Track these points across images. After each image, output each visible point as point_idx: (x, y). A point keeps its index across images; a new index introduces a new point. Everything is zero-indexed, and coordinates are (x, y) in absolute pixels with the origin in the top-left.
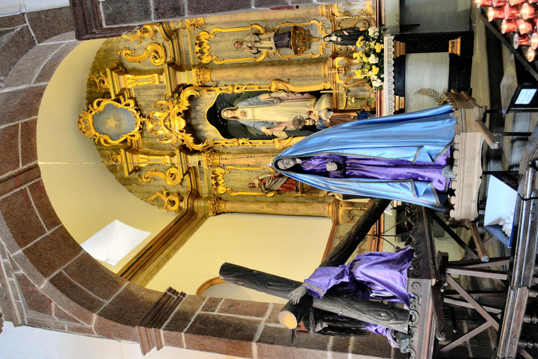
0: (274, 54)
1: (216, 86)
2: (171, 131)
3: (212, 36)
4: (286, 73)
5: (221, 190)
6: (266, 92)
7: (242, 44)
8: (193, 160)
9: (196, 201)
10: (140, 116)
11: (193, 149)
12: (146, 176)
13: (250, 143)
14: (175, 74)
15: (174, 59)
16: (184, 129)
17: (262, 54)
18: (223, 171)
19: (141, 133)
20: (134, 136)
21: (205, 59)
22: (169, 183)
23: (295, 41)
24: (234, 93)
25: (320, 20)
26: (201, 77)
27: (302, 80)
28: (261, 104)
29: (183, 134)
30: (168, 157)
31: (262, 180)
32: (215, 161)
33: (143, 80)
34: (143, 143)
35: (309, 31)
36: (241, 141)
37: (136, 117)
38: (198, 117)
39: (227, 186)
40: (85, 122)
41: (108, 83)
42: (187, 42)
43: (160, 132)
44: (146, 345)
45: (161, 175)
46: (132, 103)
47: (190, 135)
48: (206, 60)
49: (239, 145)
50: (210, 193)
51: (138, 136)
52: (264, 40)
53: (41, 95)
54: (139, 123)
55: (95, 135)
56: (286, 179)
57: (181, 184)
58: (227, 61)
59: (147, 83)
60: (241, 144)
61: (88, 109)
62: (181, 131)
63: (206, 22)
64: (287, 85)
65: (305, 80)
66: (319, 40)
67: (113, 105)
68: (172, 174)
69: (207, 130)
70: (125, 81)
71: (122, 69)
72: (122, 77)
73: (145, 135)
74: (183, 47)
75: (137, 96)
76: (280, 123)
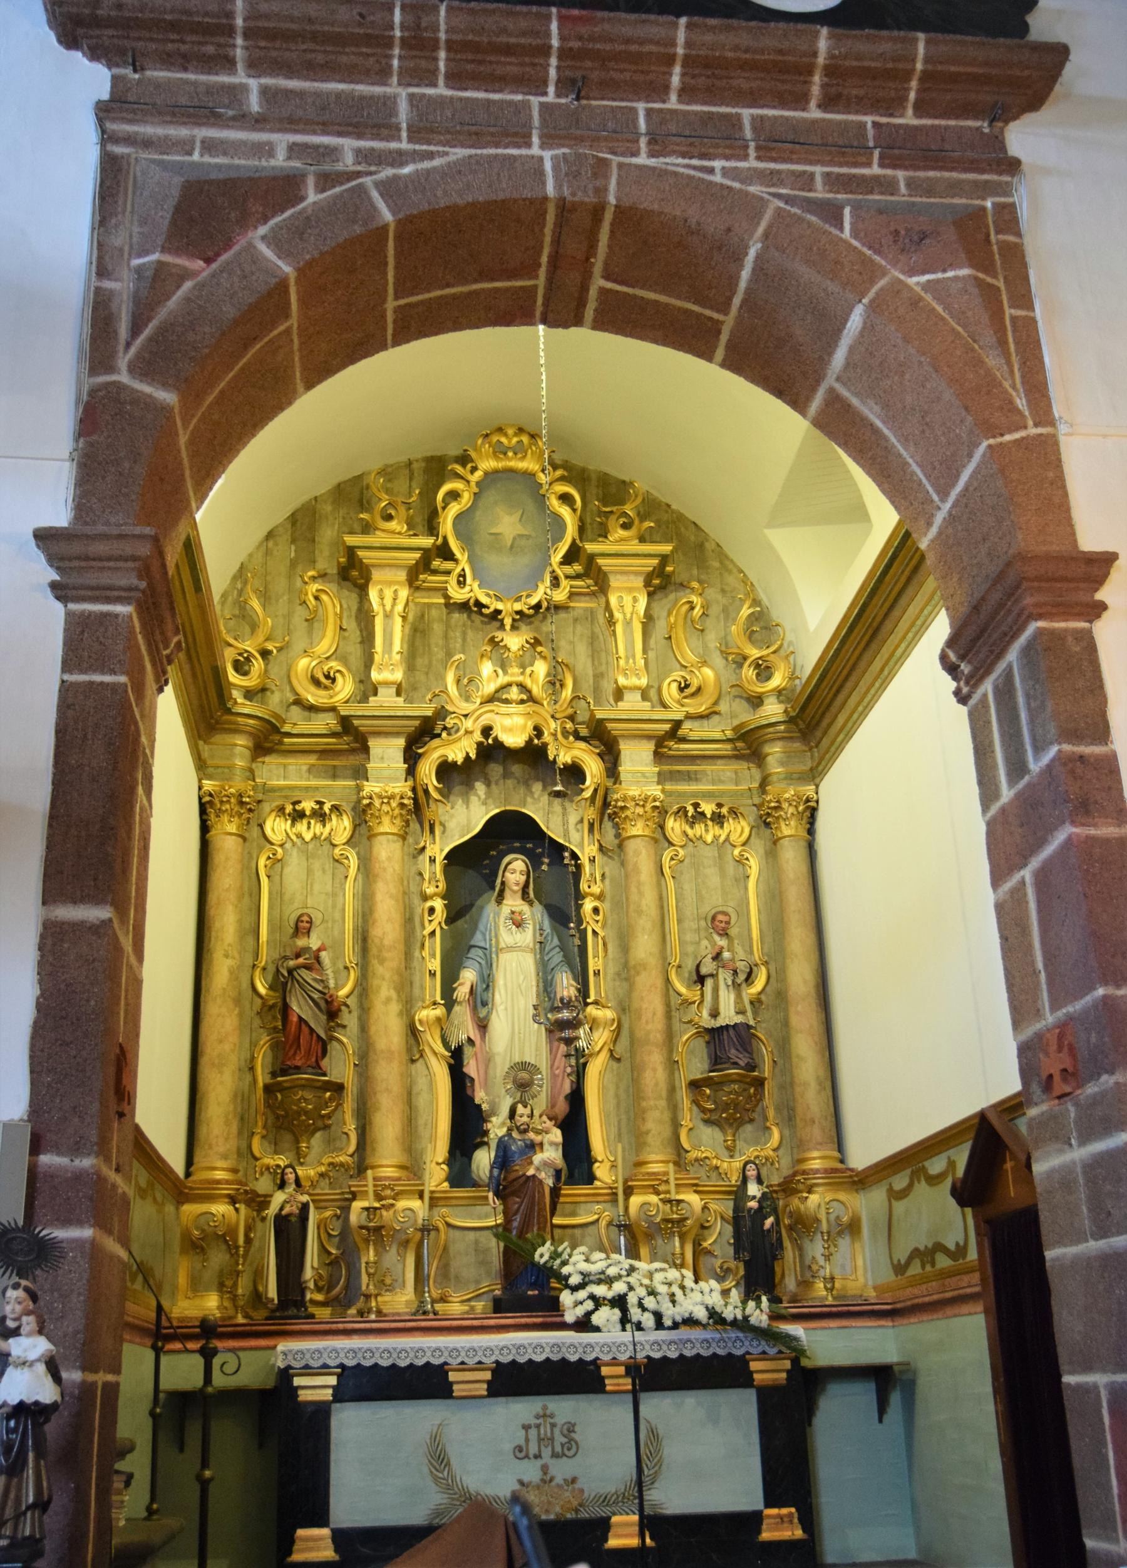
0: (690, 1022)
1: (601, 849)
2: (491, 699)
3: (736, 852)
5: (276, 828)
6: (584, 992)
7: (724, 934)
8: (387, 754)
9: (250, 744)
11: (420, 756)
12: (324, 597)
13: (433, 933)
14: (649, 737)
15: (684, 740)
16: (496, 739)
17: (688, 987)
18: (341, 837)
19: (464, 606)
20: (462, 582)
21: (677, 825)
22: (303, 663)
23: (733, 1081)
25: (781, 1152)
26: (640, 810)
27: (617, 1096)
28: (545, 973)
29: (478, 737)
30: (398, 675)
31: (318, 959)
32: (386, 820)
33: (628, 641)
34: (429, 605)
35: (751, 1121)
36: (438, 904)
37: (518, 599)
38: (510, 783)
39: (288, 845)
41: (622, 540)
42: (721, 782)
44: (77, 548)
45: (325, 645)
46: (560, 596)
47: (473, 756)
48: (674, 826)
49: (425, 898)
50: (267, 790)
51: (458, 595)
52: (739, 996)
53: (779, 393)
54: (500, 606)
57: (298, 702)
58: (671, 883)
59: (622, 652)
60: (429, 904)
62: (487, 731)
63: (785, 842)
64: (604, 1056)
65: (618, 1105)
66: (728, 1148)
68: (334, 680)
69: (471, 806)
70: (630, 590)
71: (660, 583)
72: (639, 582)
73: (456, 615)
74: (708, 768)
75: (573, 614)
76: (483, 1026)
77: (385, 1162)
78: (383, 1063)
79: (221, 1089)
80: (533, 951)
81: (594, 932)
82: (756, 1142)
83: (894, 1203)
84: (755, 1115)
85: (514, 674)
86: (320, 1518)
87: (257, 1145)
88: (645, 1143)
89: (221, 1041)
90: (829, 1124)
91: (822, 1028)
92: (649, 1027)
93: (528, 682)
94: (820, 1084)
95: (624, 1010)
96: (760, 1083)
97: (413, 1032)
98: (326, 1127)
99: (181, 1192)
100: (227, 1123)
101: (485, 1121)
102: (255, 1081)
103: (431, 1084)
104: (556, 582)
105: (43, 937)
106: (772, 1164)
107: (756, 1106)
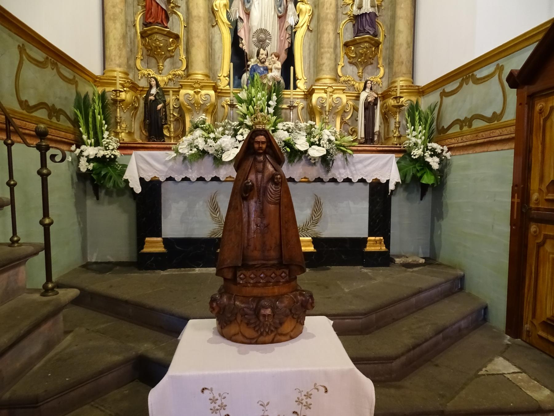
0: (346, 14)
4: (327, 24)
23: (366, 42)
25: (383, 79)
27: (309, 49)
35: (372, 64)
56: (164, 7)
64: (305, 27)
65: (310, 53)
66: (359, 76)
76: (248, 13)
77: (197, 72)
78: (195, 22)
79: (116, 31)
82: (372, 75)
83: (444, 97)
84: (373, 61)
86: (159, 235)
87: (139, 63)
88: (321, 70)
89: (114, 7)
90: (410, 65)
91: (412, 17)
92: (328, 11)
94: (408, 44)
95: (315, 6)
96: (377, 44)
97: (213, 12)
98: (172, 57)
99: (95, 80)
100: (120, 49)
101: (248, 61)
102: (136, 32)
103: (221, 39)
106: (379, 85)
107: (374, 57)
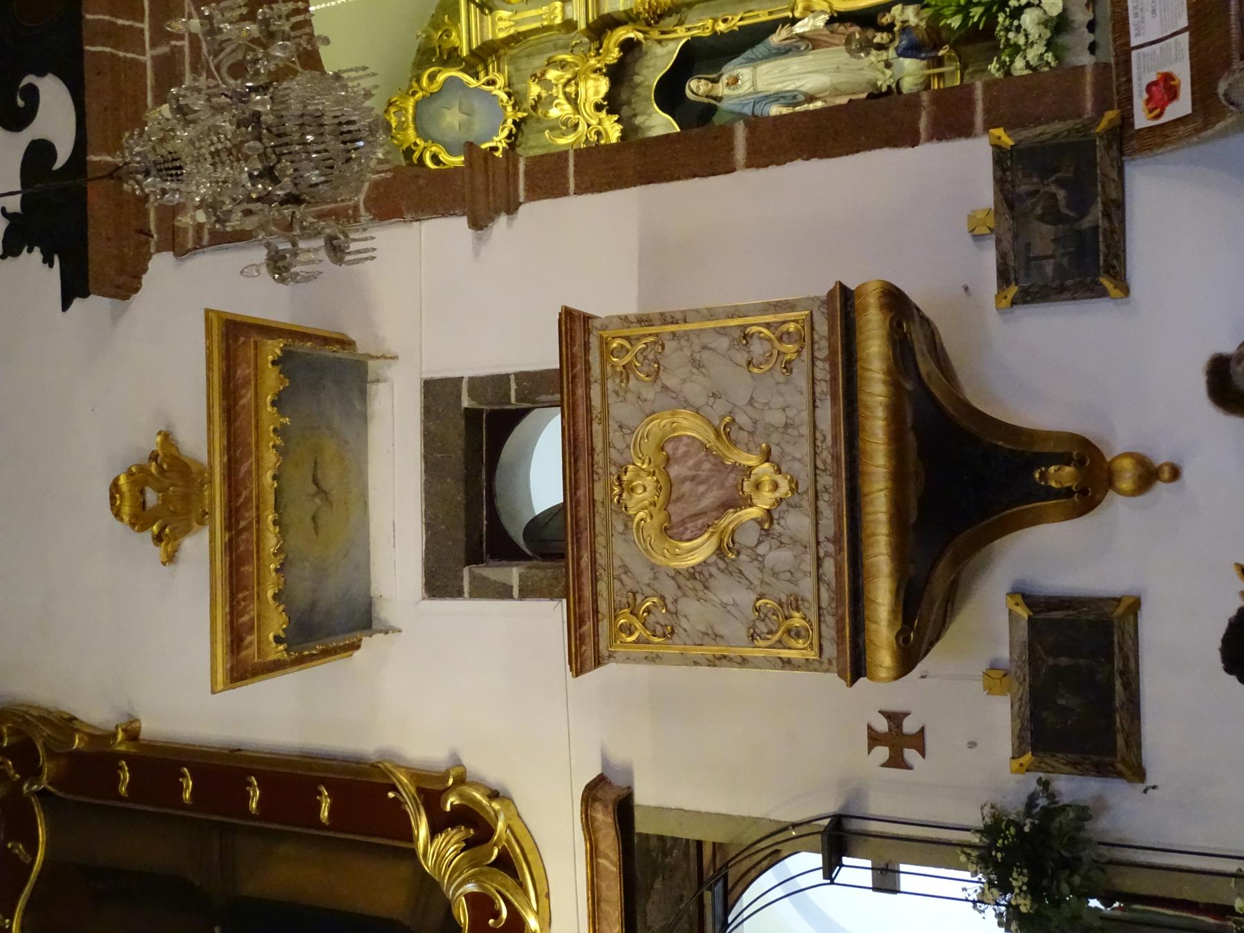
2: (577, 109)
10: (514, 106)
16: (604, 99)
24: (716, 33)
29: (603, 114)
37: (505, 108)
40: (401, 111)
43: (554, 113)
46: (501, 81)
47: (616, 117)
54: (510, 121)
55: (415, 144)
61: (411, 87)
62: (598, 107)
67: (461, 80)
70: (494, 24)
80: (755, 67)
81: (741, 19)
85: (558, 91)
93: (563, 81)
104: (492, 83)
105: (758, 166)
